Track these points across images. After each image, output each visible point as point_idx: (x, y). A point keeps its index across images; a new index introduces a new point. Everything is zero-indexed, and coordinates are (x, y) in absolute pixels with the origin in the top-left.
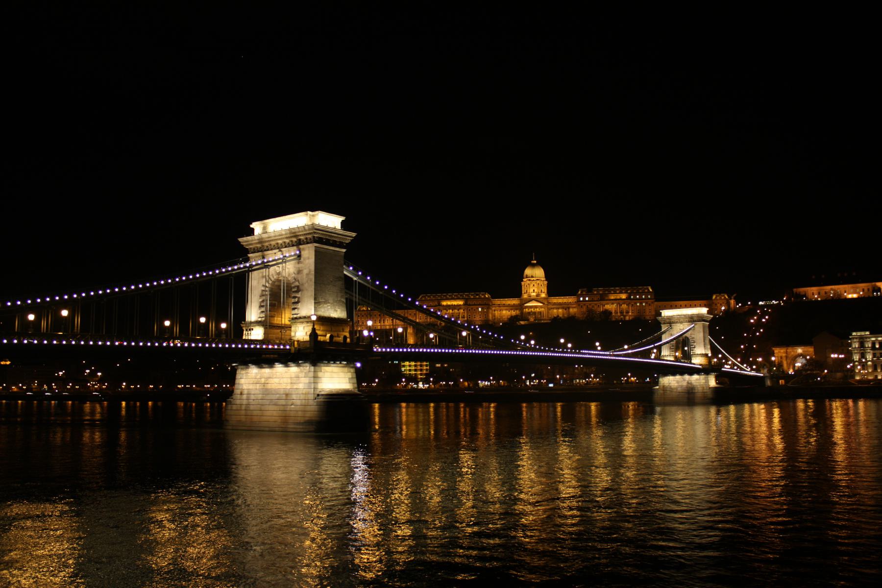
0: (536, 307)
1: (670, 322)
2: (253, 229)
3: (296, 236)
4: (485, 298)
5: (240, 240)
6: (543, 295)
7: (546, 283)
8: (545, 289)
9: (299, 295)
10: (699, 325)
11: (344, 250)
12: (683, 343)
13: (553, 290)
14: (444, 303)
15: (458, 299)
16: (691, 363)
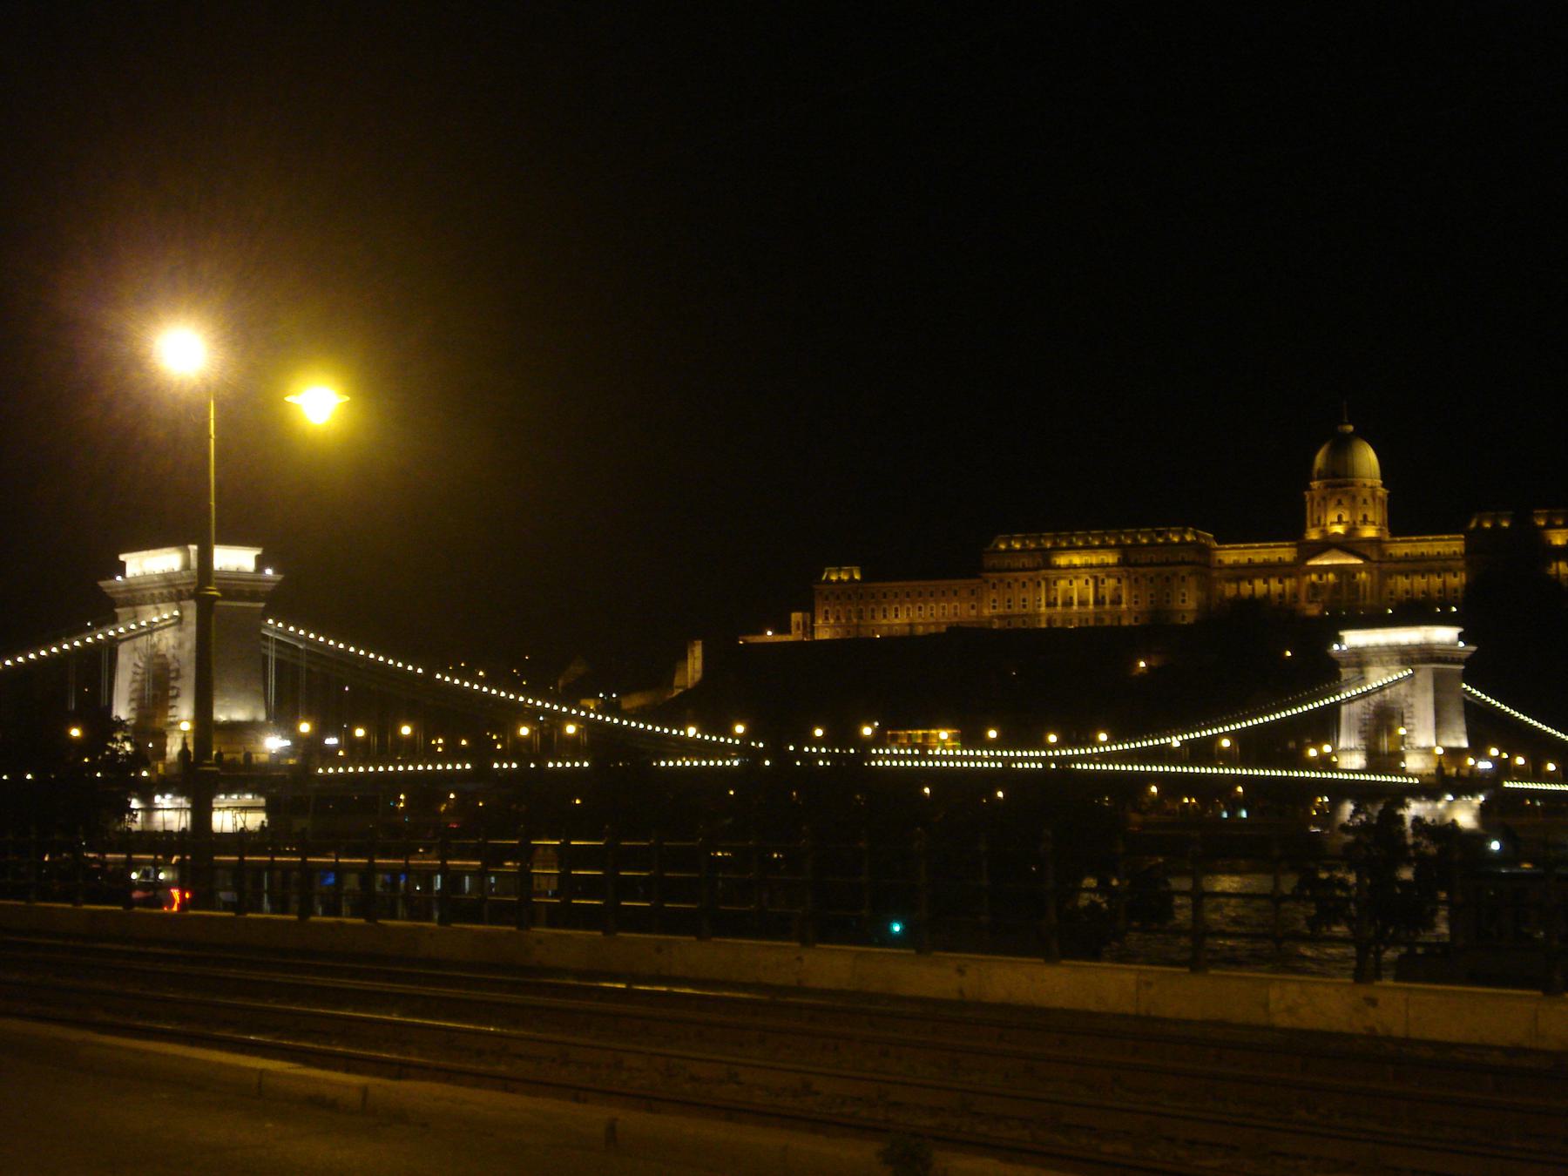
0: (1339, 570)
1: (1360, 659)
2: (123, 564)
3: (173, 586)
4: (1183, 542)
5: (102, 584)
6: (1369, 532)
7: (1382, 492)
8: (1376, 513)
9: (177, 684)
10: (1426, 672)
11: (262, 605)
12: (1383, 719)
13: (1401, 521)
14: (1062, 561)
15: (1104, 546)
16: (1402, 772)
